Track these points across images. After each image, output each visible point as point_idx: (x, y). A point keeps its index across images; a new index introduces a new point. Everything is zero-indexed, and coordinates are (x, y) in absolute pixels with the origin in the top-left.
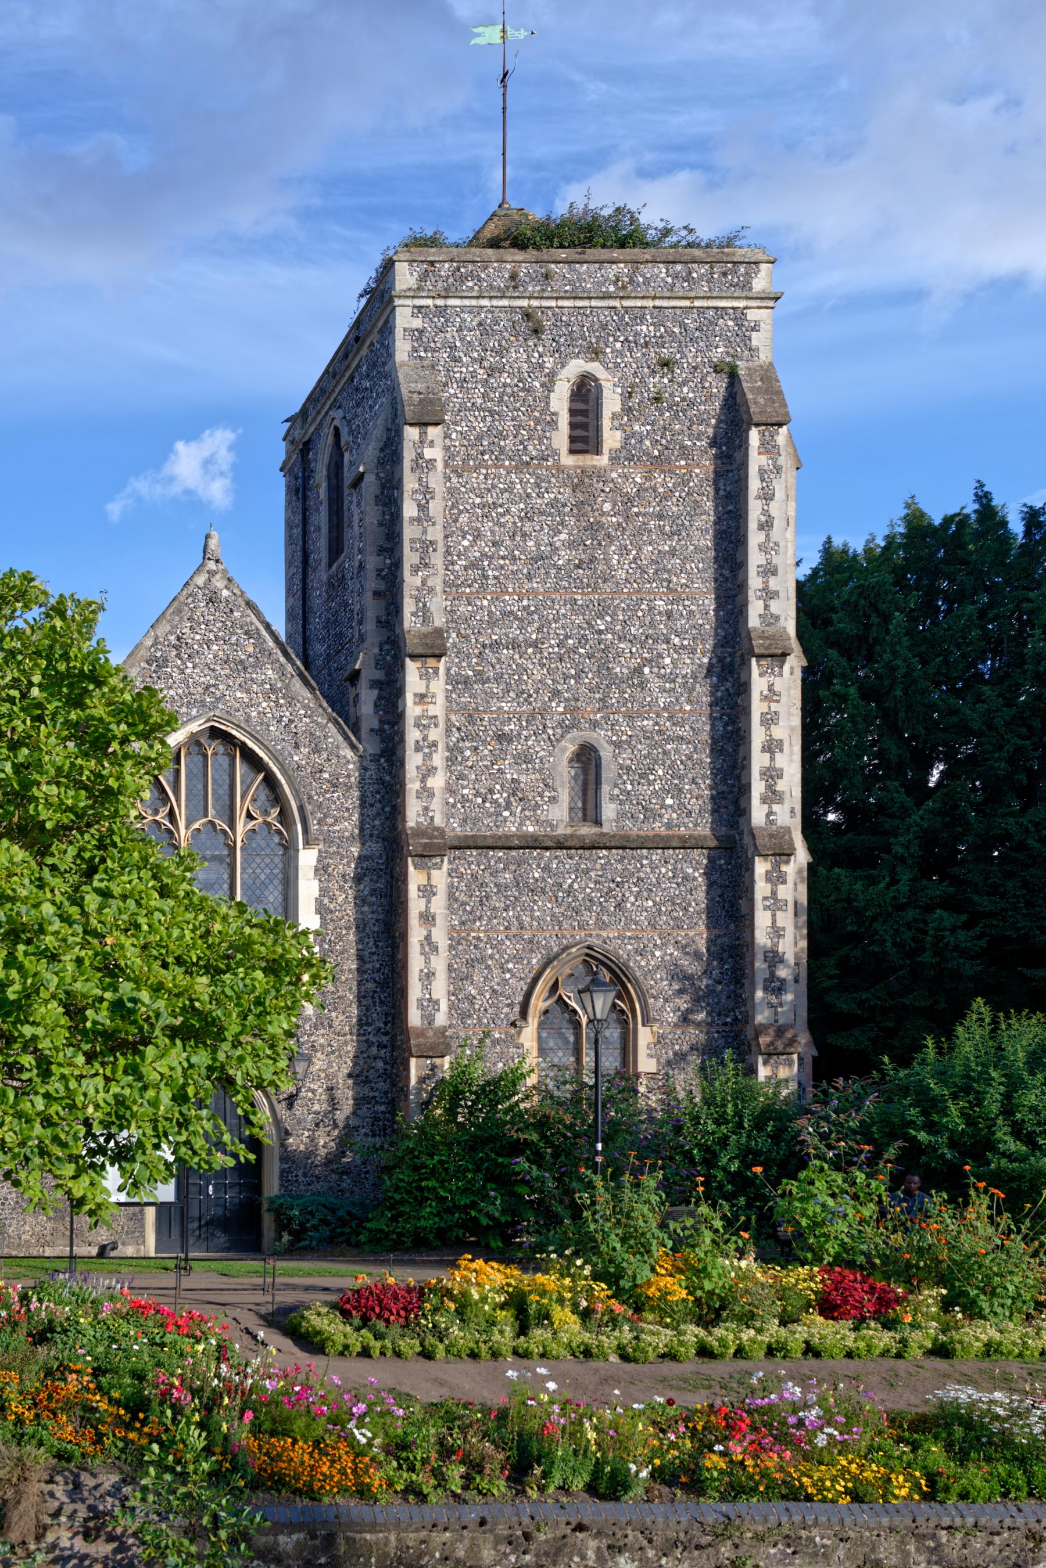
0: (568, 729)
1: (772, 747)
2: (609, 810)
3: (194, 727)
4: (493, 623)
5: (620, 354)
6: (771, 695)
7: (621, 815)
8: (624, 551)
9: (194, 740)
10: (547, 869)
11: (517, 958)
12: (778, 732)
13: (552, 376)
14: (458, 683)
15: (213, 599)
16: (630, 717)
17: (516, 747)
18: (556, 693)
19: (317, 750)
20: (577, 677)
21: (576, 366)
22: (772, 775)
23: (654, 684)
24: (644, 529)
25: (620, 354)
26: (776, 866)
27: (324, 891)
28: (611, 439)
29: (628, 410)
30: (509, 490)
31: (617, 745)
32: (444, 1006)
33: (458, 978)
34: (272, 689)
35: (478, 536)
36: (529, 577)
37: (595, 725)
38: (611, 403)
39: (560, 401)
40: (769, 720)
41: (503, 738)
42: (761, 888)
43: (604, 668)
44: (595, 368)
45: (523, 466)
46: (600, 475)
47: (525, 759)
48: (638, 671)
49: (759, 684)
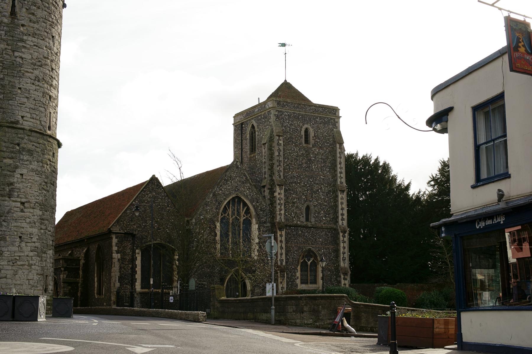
0: (305, 202)
1: (342, 209)
2: (313, 220)
3: (234, 196)
4: (291, 178)
5: (313, 124)
6: (342, 198)
7: (316, 221)
8: (315, 165)
9: (233, 198)
10: (302, 231)
11: (296, 251)
12: (343, 206)
13: (302, 127)
14: (286, 191)
15: (237, 167)
16: (317, 201)
17: (296, 205)
18: (303, 194)
19: (258, 202)
20: (307, 190)
21: (306, 126)
22: (342, 215)
23: (321, 194)
24: (318, 161)
25: (313, 124)
26: (344, 234)
27: (260, 234)
28: (312, 141)
29: (315, 136)
30: (294, 150)
31: (315, 206)
32: (284, 261)
33: (286, 254)
34: (249, 188)
35: (288, 159)
36: (298, 169)
37: (310, 201)
38: (312, 134)
39: (303, 133)
40: (342, 203)
41: (294, 203)
42: (341, 238)
43: (312, 189)
44: (309, 127)
45: (296, 146)
46: (311, 148)
47: (297, 207)
48: (318, 190)
49: (340, 196)
